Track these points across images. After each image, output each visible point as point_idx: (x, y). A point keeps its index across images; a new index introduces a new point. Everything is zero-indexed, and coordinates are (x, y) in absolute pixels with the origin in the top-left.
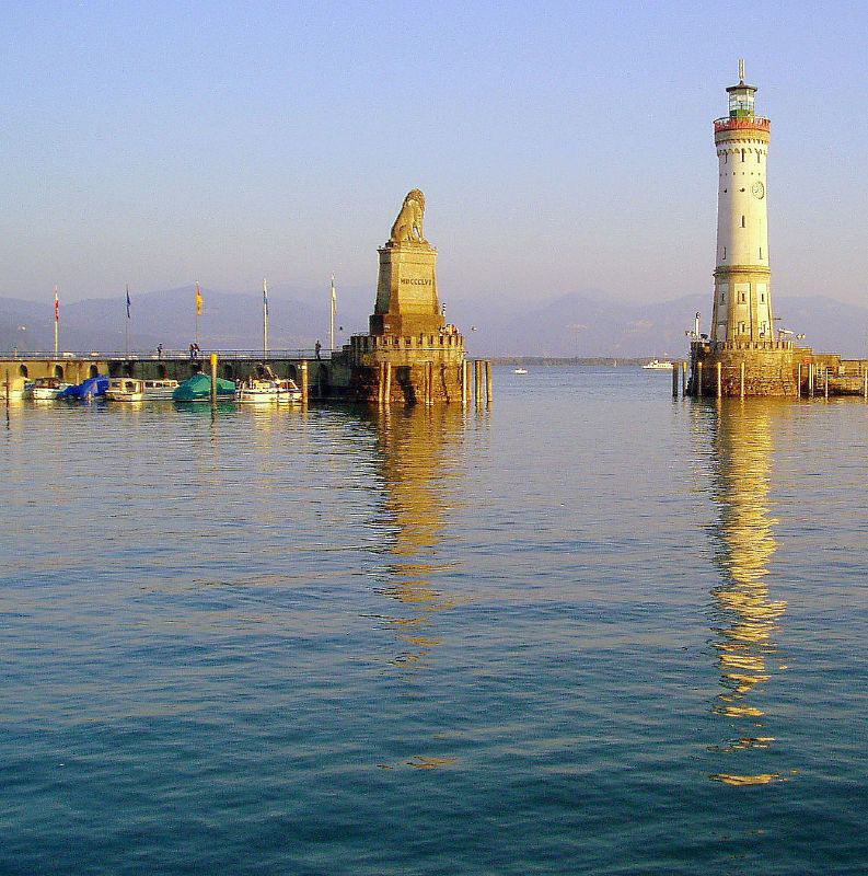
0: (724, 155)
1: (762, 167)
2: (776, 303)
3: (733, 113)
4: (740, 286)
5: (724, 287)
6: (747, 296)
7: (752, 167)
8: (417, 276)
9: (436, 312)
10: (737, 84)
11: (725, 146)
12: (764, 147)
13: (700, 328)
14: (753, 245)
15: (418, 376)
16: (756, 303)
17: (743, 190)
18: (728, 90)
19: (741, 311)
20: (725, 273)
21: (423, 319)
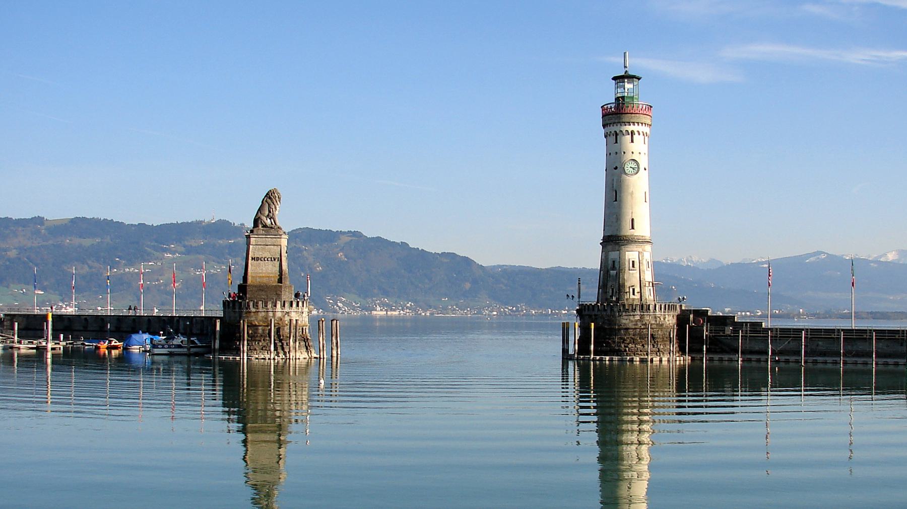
0: (606, 137)
1: (644, 149)
2: (657, 266)
3: (617, 99)
4: (631, 254)
5: (613, 255)
6: (637, 265)
7: (637, 148)
8: (268, 255)
9: (280, 281)
10: (623, 74)
11: (613, 129)
12: (646, 129)
13: (591, 296)
14: (640, 216)
15: (675, 347)
16: (640, 270)
17: (616, 168)
18: (615, 79)
19: (631, 278)
20: (614, 241)
21: (263, 288)
